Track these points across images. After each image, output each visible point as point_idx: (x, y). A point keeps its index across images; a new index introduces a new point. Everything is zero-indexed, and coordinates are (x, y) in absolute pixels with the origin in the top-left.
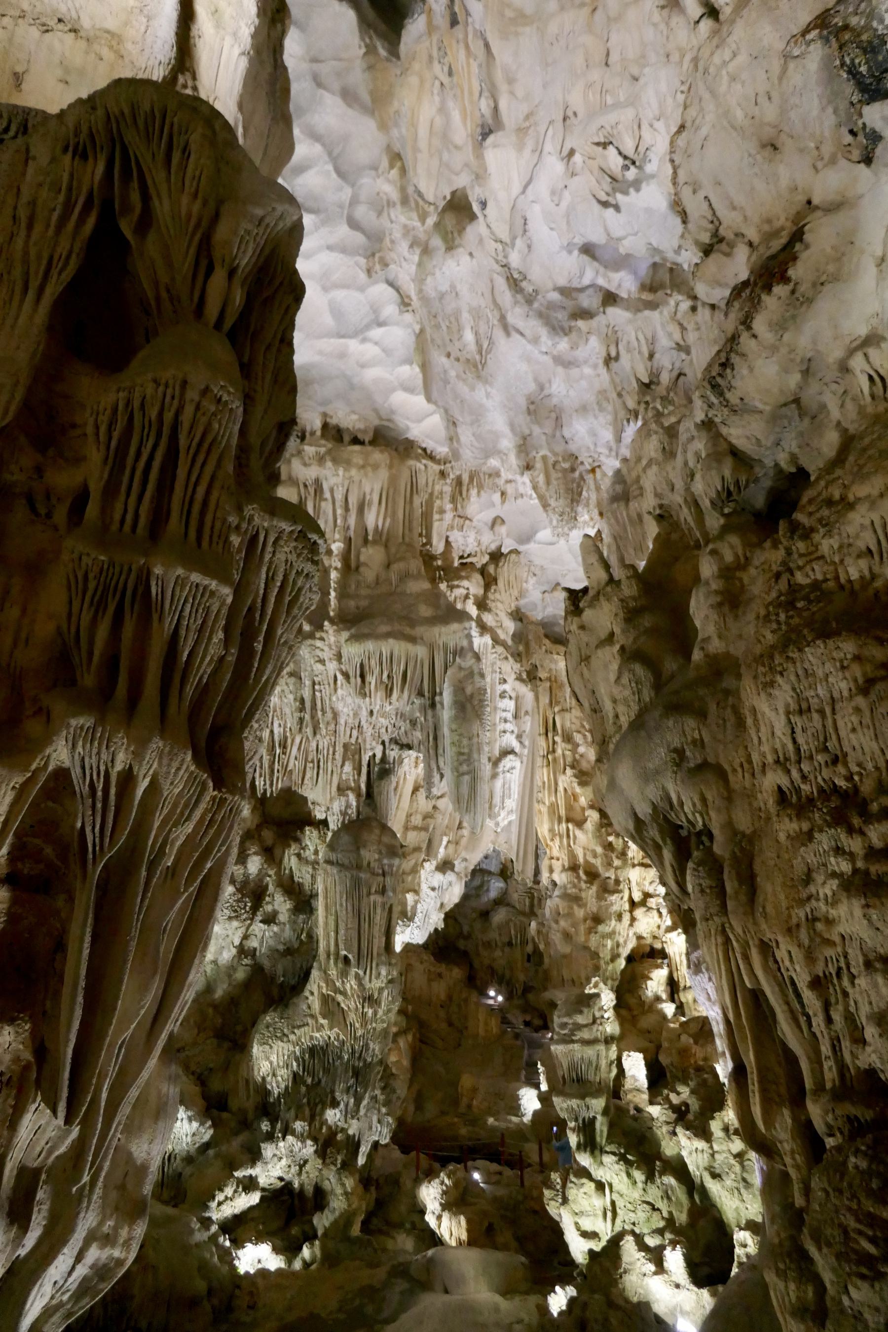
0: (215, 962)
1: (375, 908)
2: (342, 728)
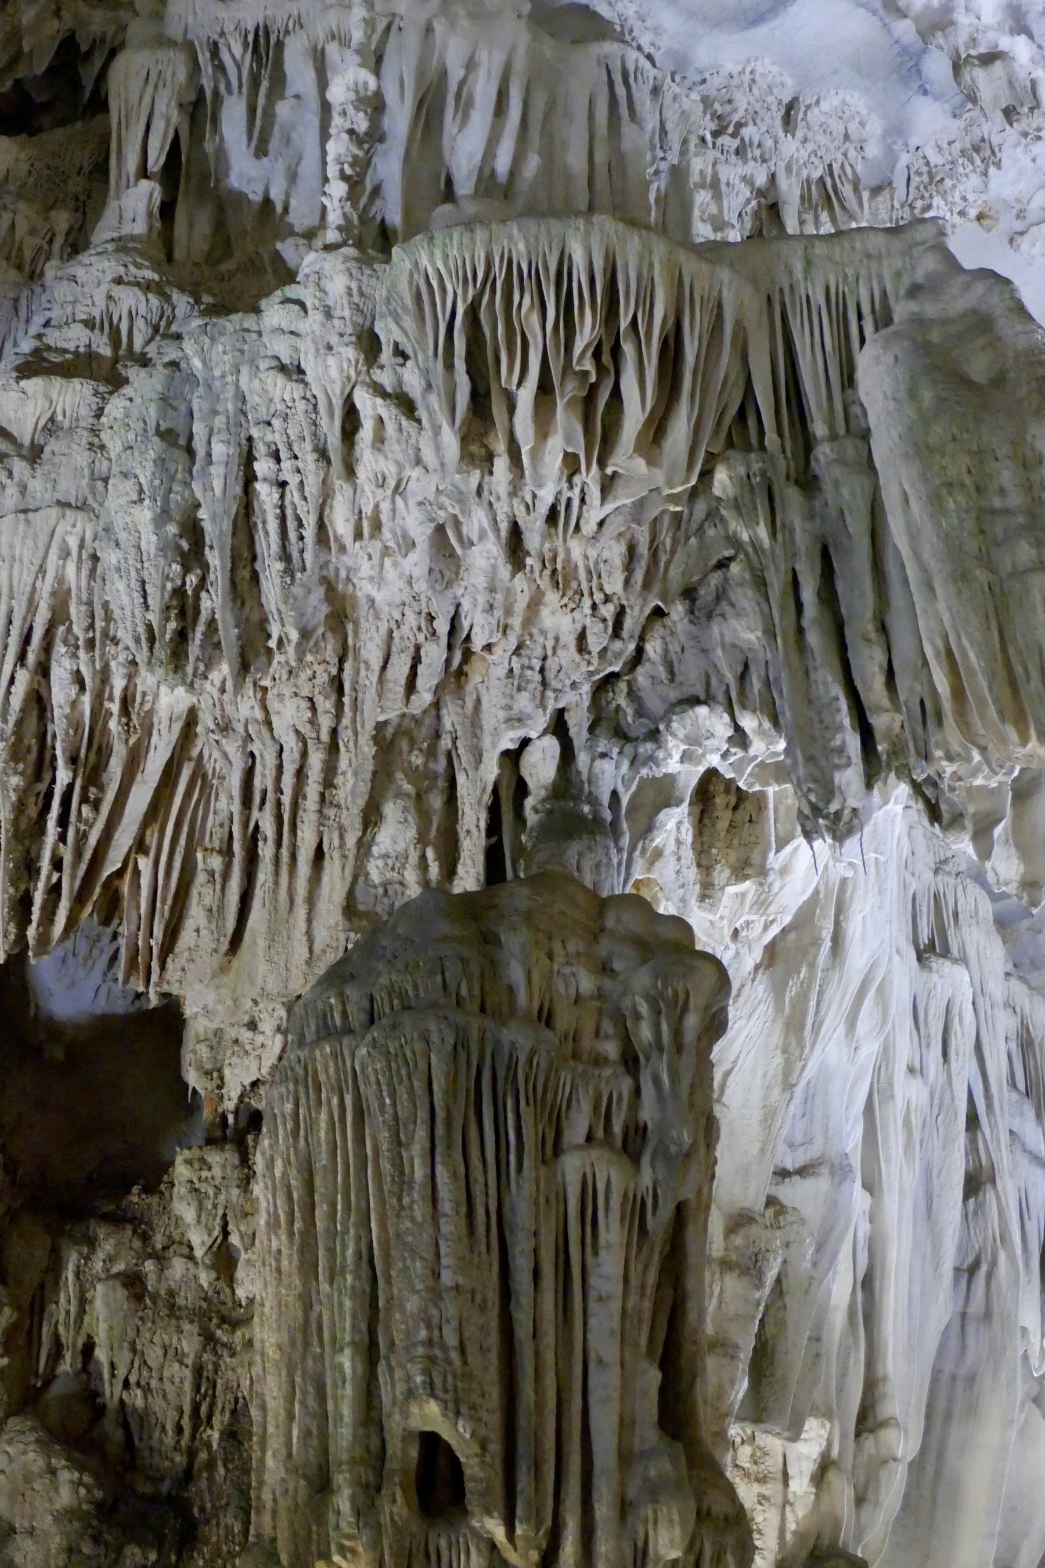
1: (590, 1221)
2: (370, 679)
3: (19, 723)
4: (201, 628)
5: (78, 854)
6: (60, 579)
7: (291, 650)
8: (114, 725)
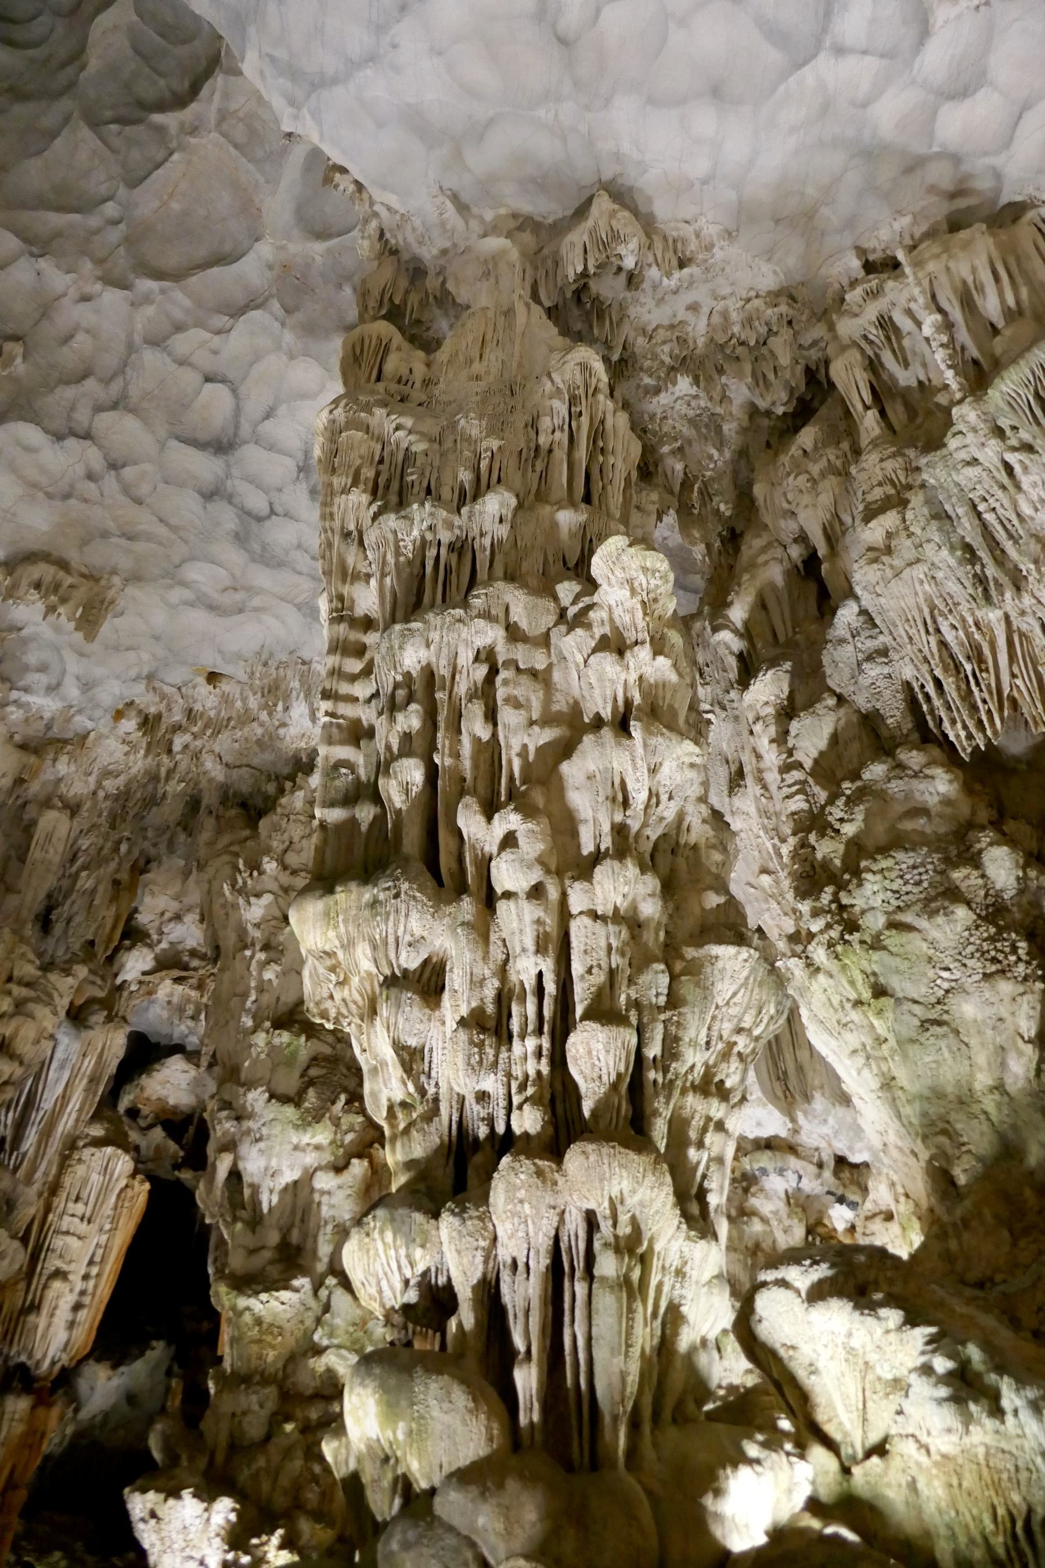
0: (999, 1087)
3: (940, 657)
4: (992, 584)
5: (990, 693)
6: (925, 593)
7: (1034, 572)
8: (977, 636)
